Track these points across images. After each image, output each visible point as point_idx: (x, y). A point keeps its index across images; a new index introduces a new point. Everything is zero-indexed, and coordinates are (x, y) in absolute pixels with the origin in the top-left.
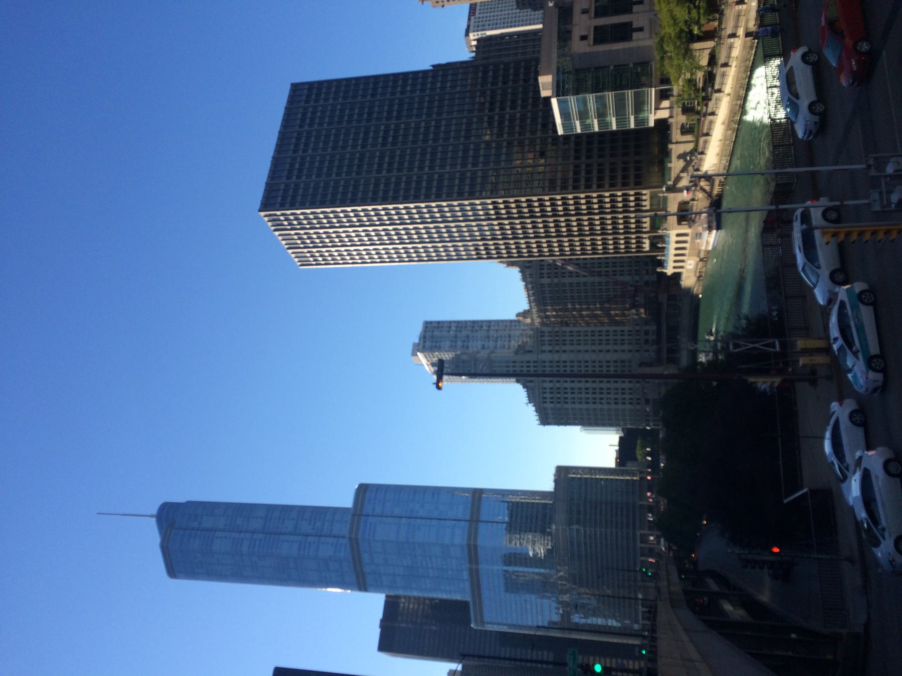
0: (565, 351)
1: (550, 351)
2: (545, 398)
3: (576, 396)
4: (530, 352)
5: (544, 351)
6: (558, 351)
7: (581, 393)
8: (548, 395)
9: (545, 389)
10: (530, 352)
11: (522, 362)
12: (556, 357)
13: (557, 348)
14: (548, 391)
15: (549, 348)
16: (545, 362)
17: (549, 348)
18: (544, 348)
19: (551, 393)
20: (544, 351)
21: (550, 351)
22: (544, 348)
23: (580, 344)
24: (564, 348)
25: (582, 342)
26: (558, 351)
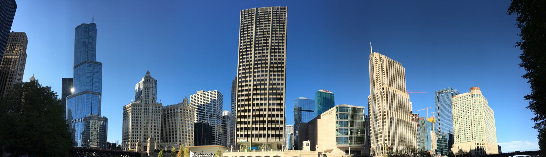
0: (152, 115)
1: (152, 109)
2: (135, 106)
3: (135, 118)
4: (153, 102)
5: (152, 107)
6: (152, 112)
7: (136, 120)
8: (136, 108)
9: (138, 107)
10: (153, 102)
11: (149, 99)
12: (150, 111)
13: (154, 112)
14: (138, 107)
15: (154, 109)
16: (148, 107)
17: (154, 109)
18: (154, 107)
19: (137, 109)
20: (152, 107)
21: (152, 109)
22: (154, 107)
23: (155, 121)
24: (153, 115)
25: (155, 116)
26: (152, 112)
